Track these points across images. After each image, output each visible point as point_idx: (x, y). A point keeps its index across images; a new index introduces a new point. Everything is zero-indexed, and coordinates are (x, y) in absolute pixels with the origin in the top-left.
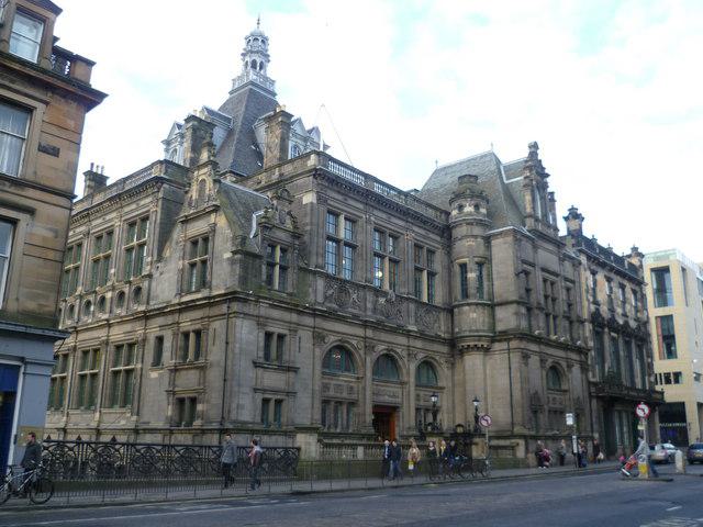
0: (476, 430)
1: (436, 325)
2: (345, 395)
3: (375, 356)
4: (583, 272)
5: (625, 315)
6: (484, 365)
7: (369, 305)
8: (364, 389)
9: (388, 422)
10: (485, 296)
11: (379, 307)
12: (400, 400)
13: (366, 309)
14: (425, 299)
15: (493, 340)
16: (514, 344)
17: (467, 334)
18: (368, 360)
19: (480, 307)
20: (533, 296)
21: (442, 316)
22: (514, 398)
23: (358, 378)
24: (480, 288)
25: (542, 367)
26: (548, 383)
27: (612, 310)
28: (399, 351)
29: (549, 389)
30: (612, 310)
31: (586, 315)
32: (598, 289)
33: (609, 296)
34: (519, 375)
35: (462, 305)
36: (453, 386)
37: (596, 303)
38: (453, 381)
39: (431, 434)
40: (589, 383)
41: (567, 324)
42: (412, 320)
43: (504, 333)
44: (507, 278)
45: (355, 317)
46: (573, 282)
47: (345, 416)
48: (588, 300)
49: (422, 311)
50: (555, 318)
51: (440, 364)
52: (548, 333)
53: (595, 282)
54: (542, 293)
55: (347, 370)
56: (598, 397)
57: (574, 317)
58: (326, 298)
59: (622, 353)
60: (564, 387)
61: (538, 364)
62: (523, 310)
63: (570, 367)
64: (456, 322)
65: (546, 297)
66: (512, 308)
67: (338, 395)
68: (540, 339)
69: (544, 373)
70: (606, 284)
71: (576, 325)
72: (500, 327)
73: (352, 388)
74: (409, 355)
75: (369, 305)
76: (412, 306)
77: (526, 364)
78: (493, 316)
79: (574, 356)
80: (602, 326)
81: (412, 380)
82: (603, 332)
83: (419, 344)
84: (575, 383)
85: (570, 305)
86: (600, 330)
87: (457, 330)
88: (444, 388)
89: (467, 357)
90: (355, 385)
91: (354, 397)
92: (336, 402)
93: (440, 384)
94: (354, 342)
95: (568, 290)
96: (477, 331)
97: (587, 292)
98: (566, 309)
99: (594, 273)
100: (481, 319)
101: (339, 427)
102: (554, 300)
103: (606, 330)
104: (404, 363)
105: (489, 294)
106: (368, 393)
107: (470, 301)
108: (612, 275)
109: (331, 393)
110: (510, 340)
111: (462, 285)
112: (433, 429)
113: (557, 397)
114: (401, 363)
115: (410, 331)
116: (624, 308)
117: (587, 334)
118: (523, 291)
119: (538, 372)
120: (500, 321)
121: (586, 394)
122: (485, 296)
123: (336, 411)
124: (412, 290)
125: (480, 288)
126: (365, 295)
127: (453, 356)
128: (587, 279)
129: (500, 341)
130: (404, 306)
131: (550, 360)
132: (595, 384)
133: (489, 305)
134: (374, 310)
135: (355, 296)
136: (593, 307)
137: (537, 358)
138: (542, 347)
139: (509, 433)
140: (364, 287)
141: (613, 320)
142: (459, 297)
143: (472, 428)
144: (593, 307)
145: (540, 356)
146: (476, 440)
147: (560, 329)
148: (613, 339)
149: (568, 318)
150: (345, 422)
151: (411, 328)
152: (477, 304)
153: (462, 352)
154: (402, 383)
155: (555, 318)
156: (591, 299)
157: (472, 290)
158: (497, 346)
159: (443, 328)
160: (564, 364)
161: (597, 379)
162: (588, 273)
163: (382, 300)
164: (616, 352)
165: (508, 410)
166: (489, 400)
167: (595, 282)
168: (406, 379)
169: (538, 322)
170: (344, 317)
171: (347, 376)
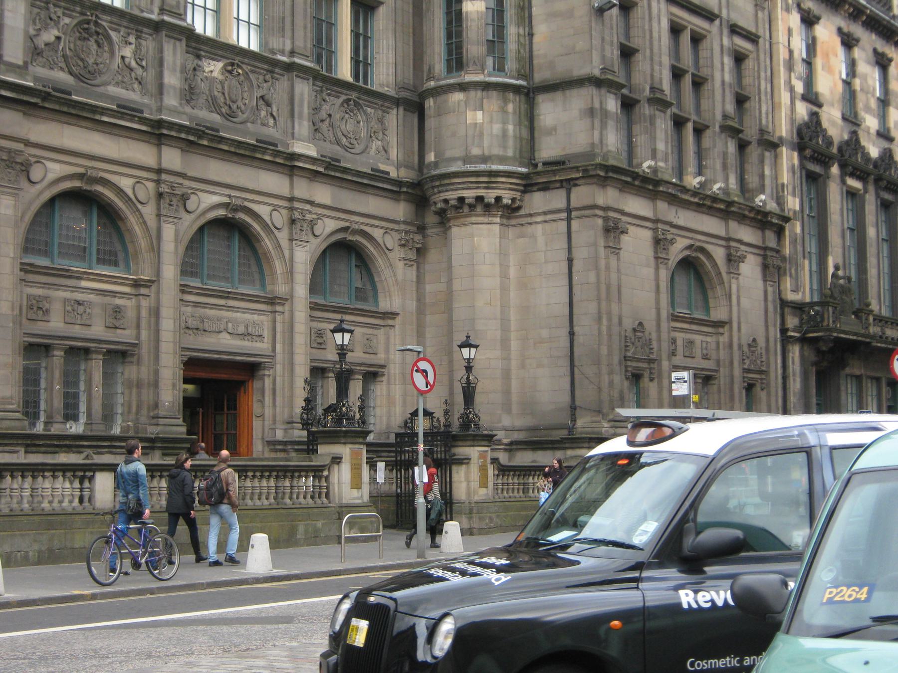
0: (467, 422)
1: (376, 144)
2: (98, 330)
3: (189, 224)
4: (780, 13)
5: (884, 135)
6: (503, 254)
7: (172, 79)
8: (156, 313)
9: (233, 406)
10: (511, 64)
11: (203, 87)
12: (262, 346)
13: (161, 88)
14: (344, 70)
15: (528, 185)
16: (582, 194)
17: (453, 169)
18: (168, 231)
19: (494, 94)
20: (641, 64)
21: (394, 118)
22: (579, 340)
23: (137, 284)
24: (496, 44)
25: (656, 258)
26: (672, 304)
27: (851, 119)
28: (263, 211)
29: (675, 318)
30: (851, 119)
31: (784, 129)
32: (819, 62)
33: (847, 83)
34: (592, 277)
35: (451, 88)
36: (421, 311)
37: (811, 97)
38: (420, 299)
39: (333, 437)
40: (784, 304)
41: (732, 147)
42: (303, 127)
43: (557, 164)
44: (569, 14)
45: (127, 110)
46: (752, 38)
47: (97, 390)
48: (792, 89)
49: (333, 104)
50: (699, 131)
51: (385, 250)
52: (680, 171)
53: (811, 46)
54: (666, 61)
55: (108, 258)
56: (803, 340)
57: (751, 133)
58: (35, 52)
59: (871, 232)
60: (718, 313)
61: (648, 251)
62: (612, 104)
63: (733, 260)
64: (430, 136)
65: (677, 74)
66: (579, 99)
67: (77, 330)
68: (657, 183)
69: (664, 275)
70: (840, 51)
71: (754, 152)
72: (548, 150)
73: (117, 311)
74: (293, 222)
75: (172, 79)
76: (304, 89)
77: (615, 250)
78: (530, 119)
79: (747, 234)
80: (824, 159)
81: (301, 291)
82: (828, 176)
83: (323, 194)
84: (745, 302)
85: (741, 100)
86: (816, 168)
87: (431, 157)
88: (393, 315)
89: (455, 231)
90: (128, 304)
91: (126, 335)
92: (72, 352)
93: (384, 305)
94: (126, 184)
95: (739, 58)
96: (485, 159)
97: (790, 66)
98: (730, 108)
99: (809, 21)
100: (497, 128)
101: (83, 419)
102: (698, 83)
103: (835, 170)
104: (278, 246)
105: (519, 59)
106: (167, 325)
107: (469, 78)
108: (858, 30)
109: (56, 324)
110: (569, 184)
111: (449, 36)
112: (338, 421)
113: (698, 338)
114: (268, 243)
115: (293, 156)
116: (883, 117)
117: (785, 178)
118: (615, 53)
119: (649, 272)
120: (552, 131)
121: (775, 333)
122: (511, 64)
123: (70, 380)
124: (304, 39)
125: (496, 44)
126: (161, 51)
127: (421, 229)
128: (790, 31)
129: (545, 187)
130: (279, 89)
131: (685, 242)
132: (799, 308)
133: (516, 89)
134: (189, 94)
135: (128, 52)
136: (802, 110)
137: (647, 235)
138: (662, 205)
139: (563, 433)
140: (157, 27)
141: (853, 144)
142: (440, 67)
143: (456, 422)
144: (802, 110)
145: (655, 230)
146: (462, 451)
147: (714, 162)
148: (851, 194)
149: (733, 131)
150: (97, 405)
151: (299, 148)
152: (486, 86)
153: (444, 218)
154: (272, 301)
155: (699, 131)
156: (799, 87)
157: (474, 48)
158: (538, 201)
159: (394, 153)
160: (719, 254)
161: (805, 295)
162: (795, 19)
163: (214, 68)
164: (858, 230)
165: (566, 370)
166: (514, 345)
167: (811, 46)
168: (281, 289)
169: (653, 139)
170: (94, 109)
171: (99, 278)
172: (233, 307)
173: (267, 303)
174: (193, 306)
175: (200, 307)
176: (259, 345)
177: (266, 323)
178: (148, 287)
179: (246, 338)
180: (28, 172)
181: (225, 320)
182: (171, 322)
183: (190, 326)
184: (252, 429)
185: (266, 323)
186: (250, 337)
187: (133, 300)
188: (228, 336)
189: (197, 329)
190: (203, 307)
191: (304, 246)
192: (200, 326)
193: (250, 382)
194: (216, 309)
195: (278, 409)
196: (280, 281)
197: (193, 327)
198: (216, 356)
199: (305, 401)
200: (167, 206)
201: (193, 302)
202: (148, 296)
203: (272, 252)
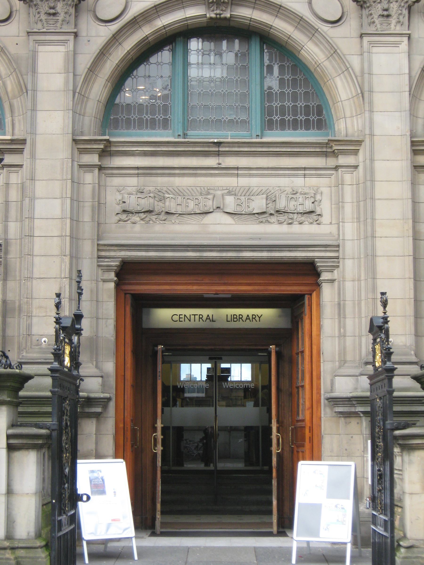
172: (237, 168)
173: (325, 154)
174: (138, 175)
175: (157, 175)
176: (313, 229)
177: (326, 191)
178: (20, 151)
179: (273, 219)
180: (94, 12)
181: (219, 193)
182: (58, 202)
183: (130, 209)
184: (319, 378)
185: (326, 191)
186: (282, 218)
187: (333, 177)
188: (228, 219)
189: (150, 212)
190: (163, 175)
191: (396, 44)
192: (159, 206)
193: (314, 294)
194: (195, 175)
195: (349, 341)
196: (348, 114)
197: (139, 208)
198: (191, 255)
199: (389, 321)
200: (43, 17)
201: (138, 168)
202: (21, 166)
203: (327, 64)
